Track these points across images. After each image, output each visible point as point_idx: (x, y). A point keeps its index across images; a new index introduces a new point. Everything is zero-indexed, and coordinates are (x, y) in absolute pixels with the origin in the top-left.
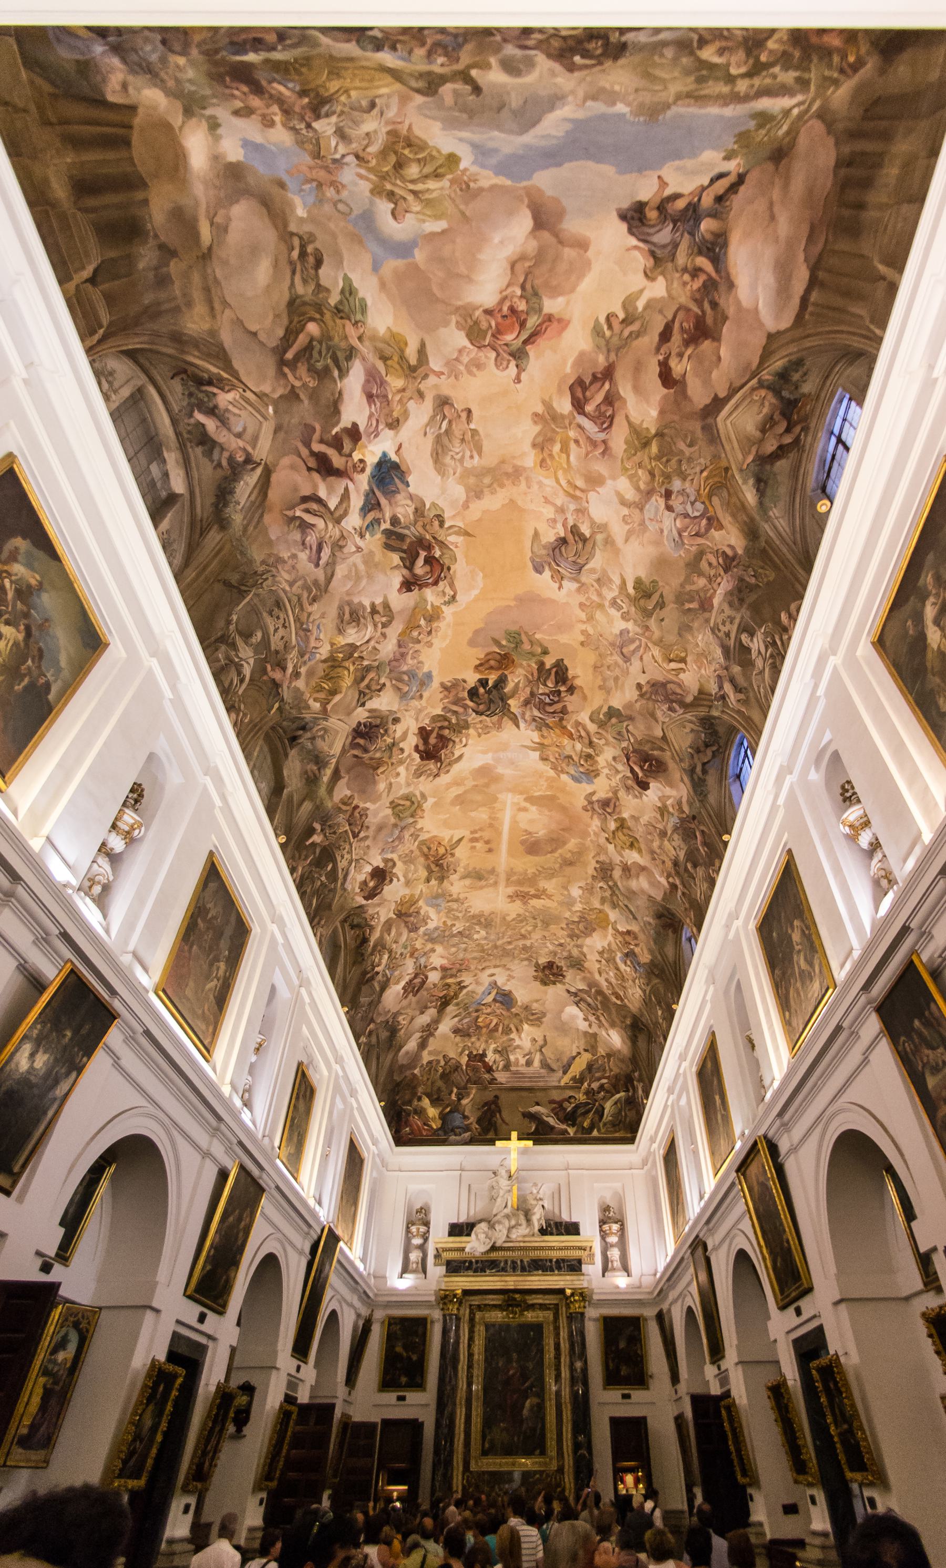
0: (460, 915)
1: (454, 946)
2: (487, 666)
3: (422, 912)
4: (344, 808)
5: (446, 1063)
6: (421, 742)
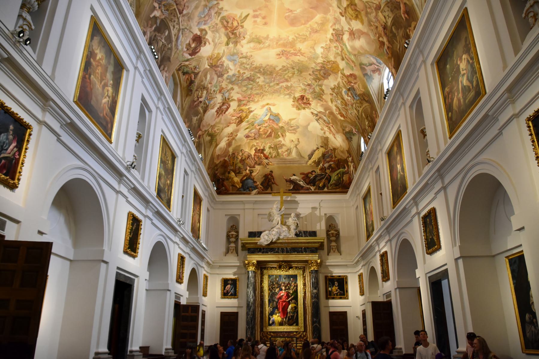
0: (248, 67)
1: (245, 86)
3: (225, 65)
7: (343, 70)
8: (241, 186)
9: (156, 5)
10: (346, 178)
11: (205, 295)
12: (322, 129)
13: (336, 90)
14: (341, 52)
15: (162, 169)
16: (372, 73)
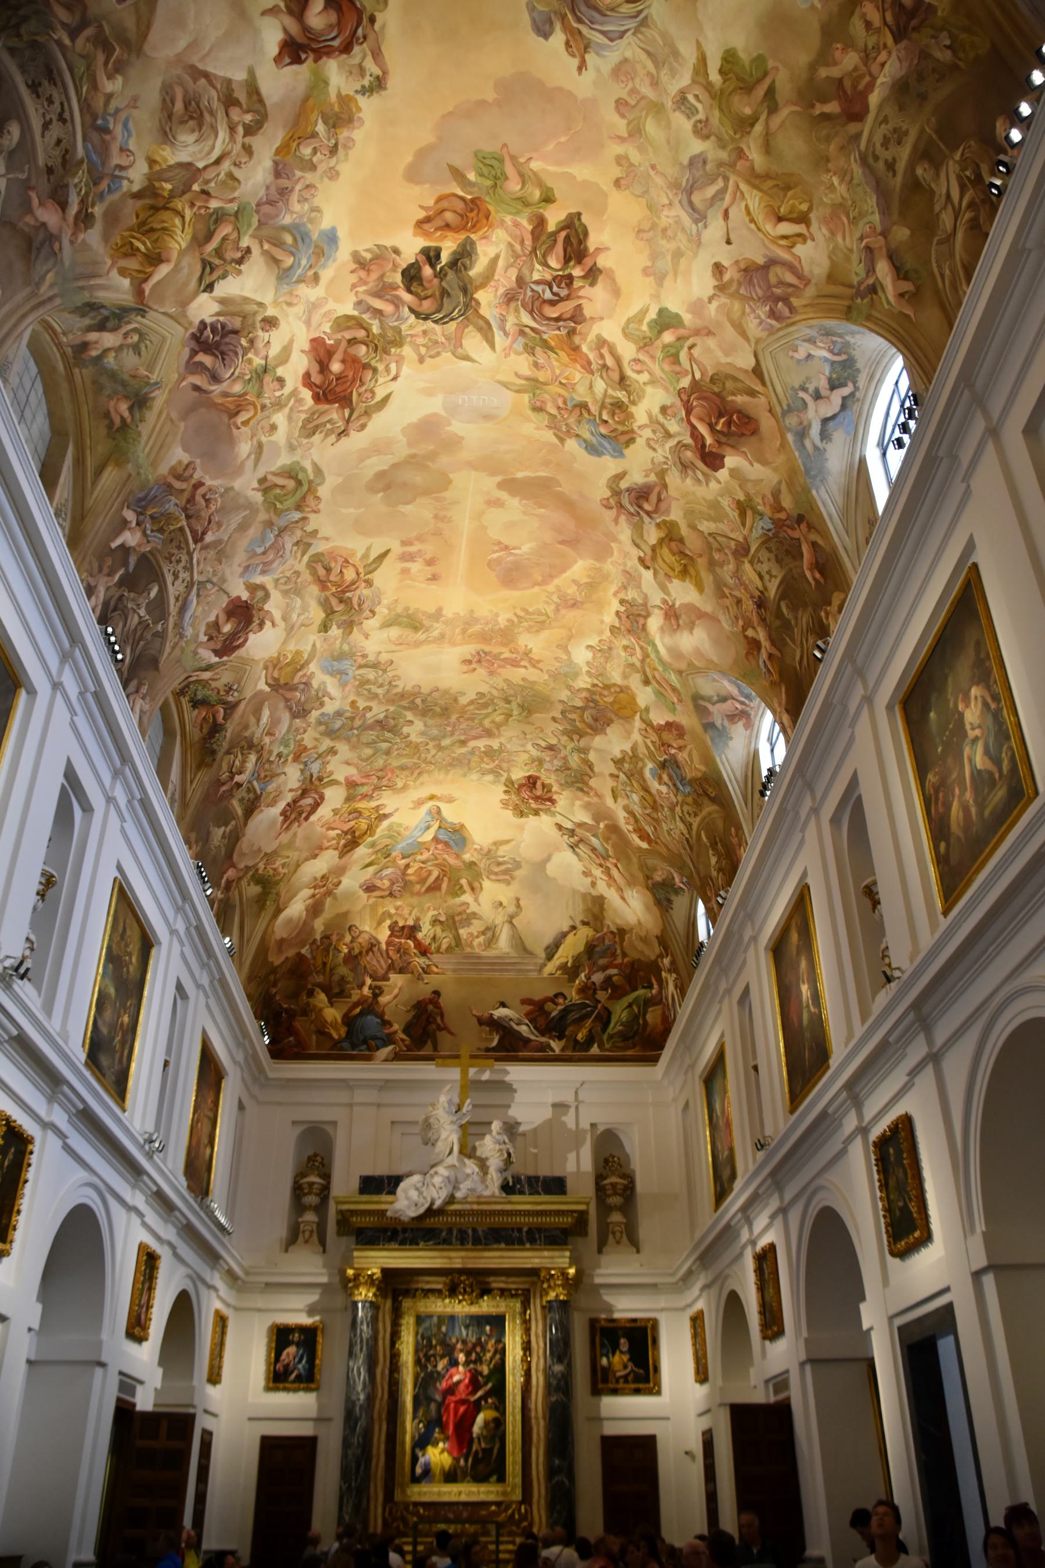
0: (380, 691)
1: (368, 745)
2: (438, 222)
3: (315, 684)
4: (177, 485)
6: (315, 369)
7: (647, 710)
8: (343, 1035)
9: (130, 515)
10: (653, 1016)
11: (214, 1378)
12: (586, 874)
13: (626, 766)
14: (643, 661)
15: (108, 981)
16: (726, 723)
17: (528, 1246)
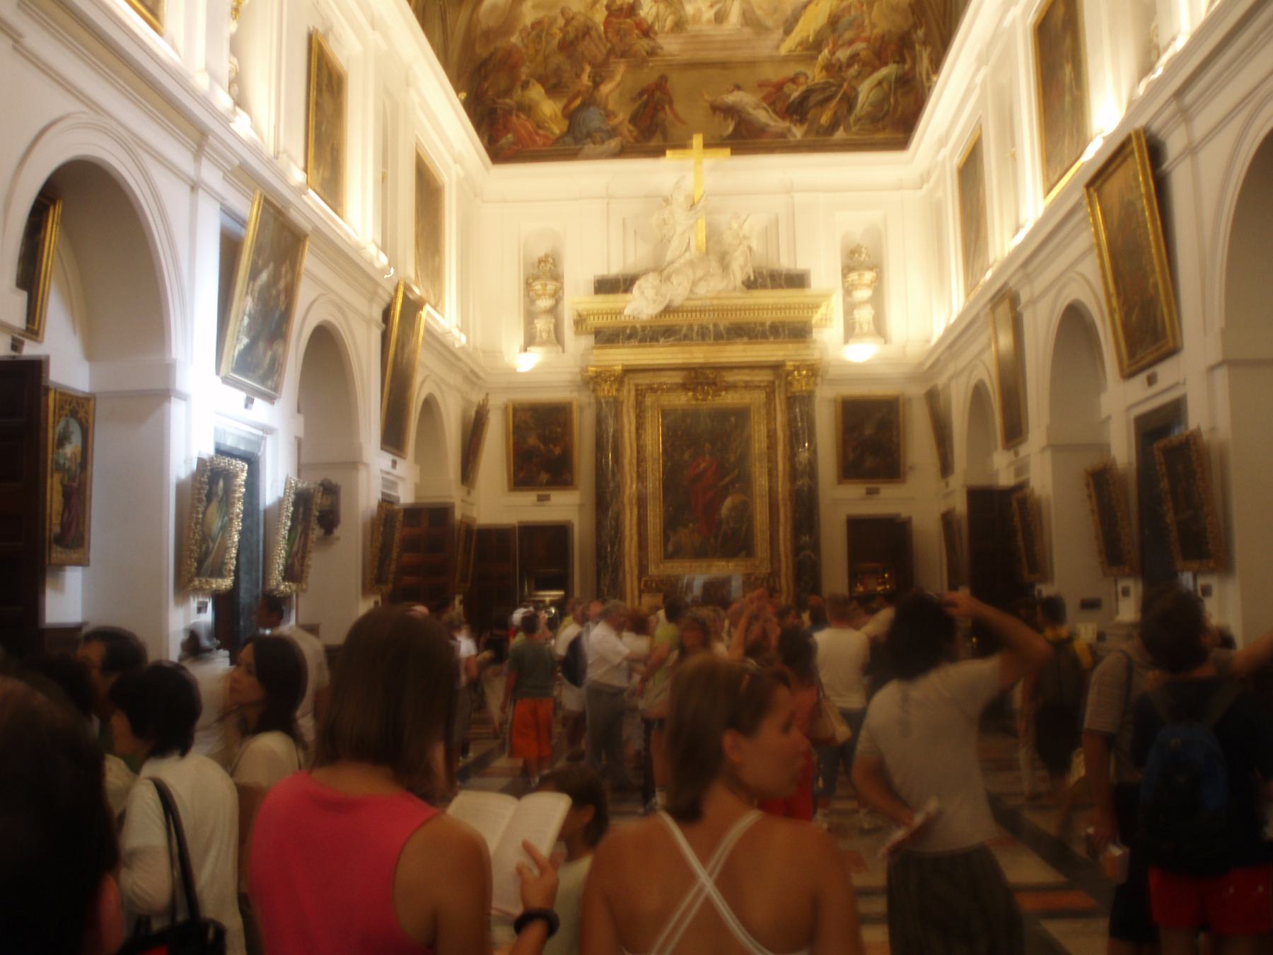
5: (568, 23)
8: (565, 128)
17: (772, 339)
